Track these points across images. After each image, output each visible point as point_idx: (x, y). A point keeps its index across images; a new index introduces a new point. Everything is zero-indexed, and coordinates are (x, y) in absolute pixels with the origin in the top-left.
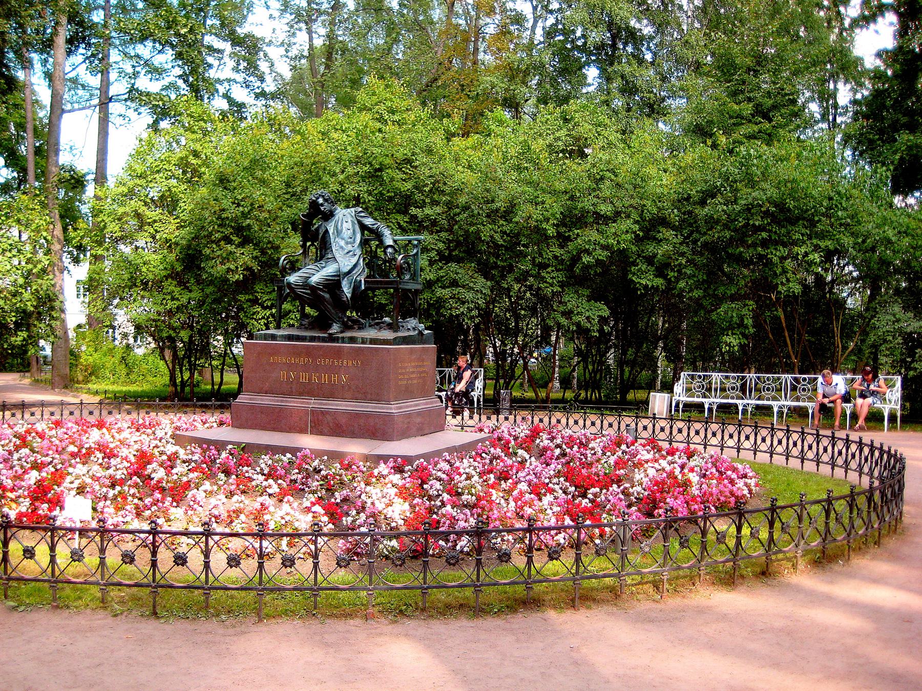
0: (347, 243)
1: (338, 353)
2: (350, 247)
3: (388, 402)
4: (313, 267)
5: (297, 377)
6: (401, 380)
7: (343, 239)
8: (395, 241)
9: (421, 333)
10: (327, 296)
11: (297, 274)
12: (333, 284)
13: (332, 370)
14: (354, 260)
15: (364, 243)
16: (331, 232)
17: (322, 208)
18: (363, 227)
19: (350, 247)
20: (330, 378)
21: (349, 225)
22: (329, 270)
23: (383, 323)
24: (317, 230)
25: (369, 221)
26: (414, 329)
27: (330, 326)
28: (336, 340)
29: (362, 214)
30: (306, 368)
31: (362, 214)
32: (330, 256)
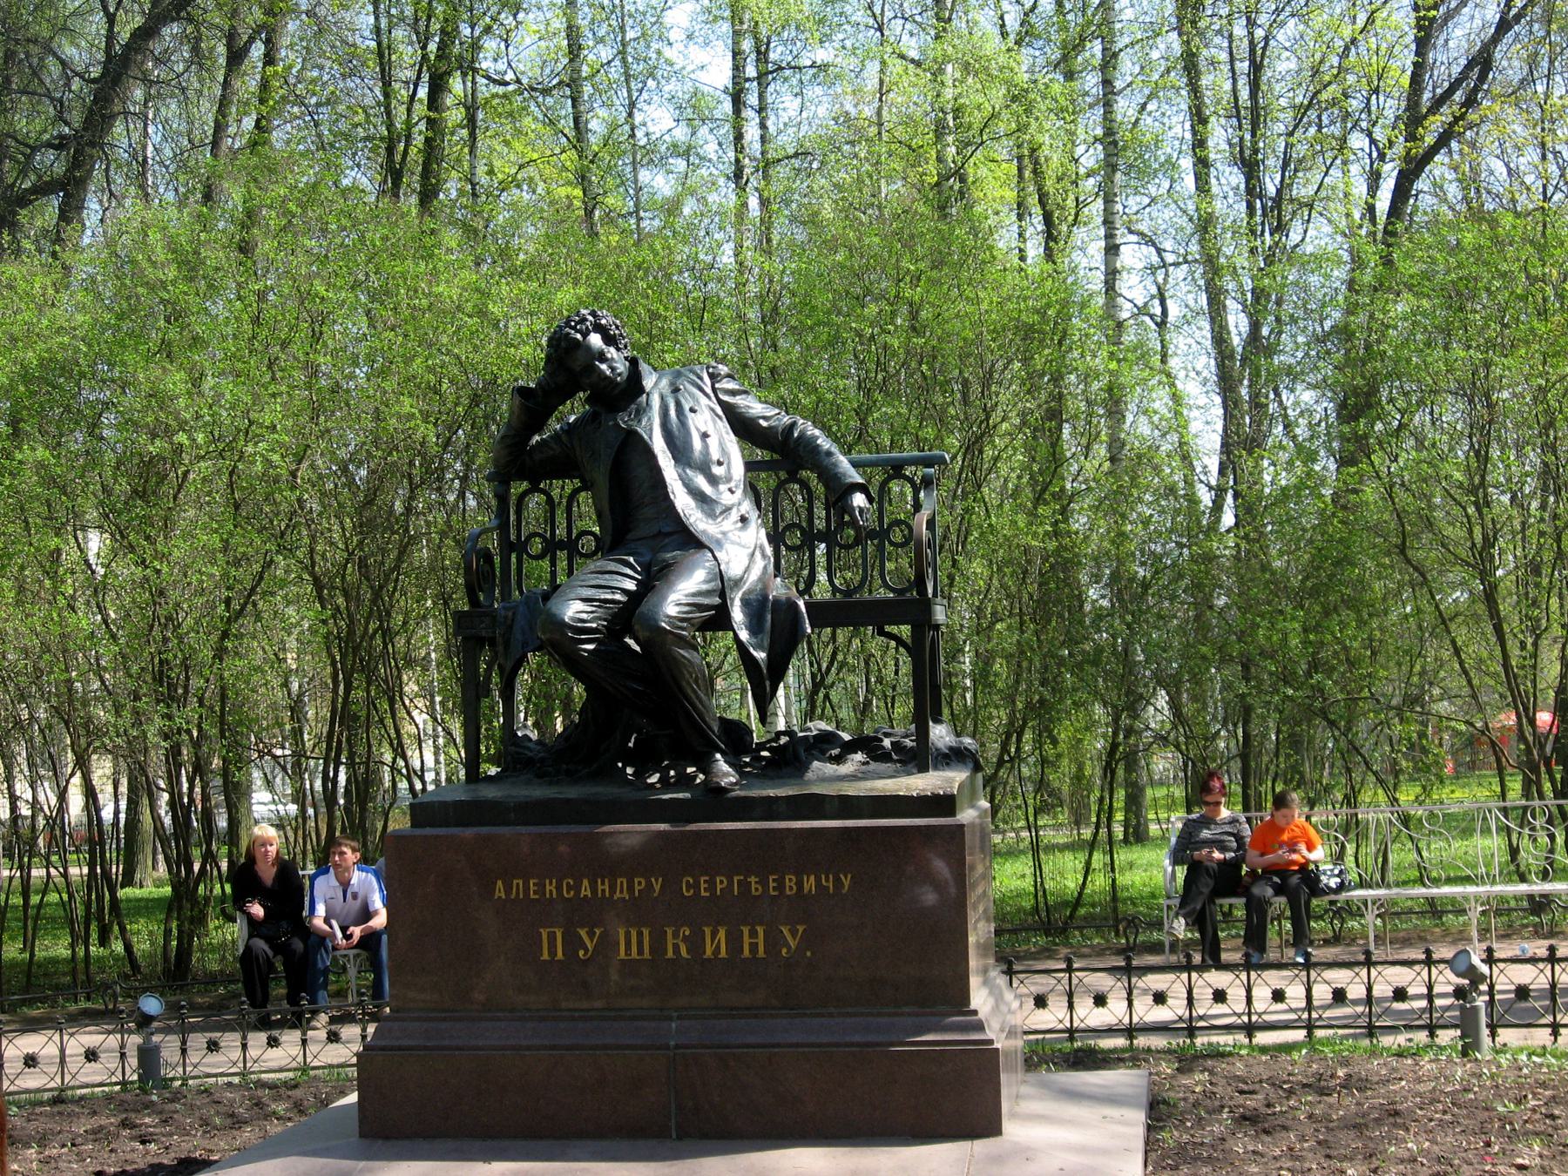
13: (737, 911)
25: (754, 407)
28: (745, 808)
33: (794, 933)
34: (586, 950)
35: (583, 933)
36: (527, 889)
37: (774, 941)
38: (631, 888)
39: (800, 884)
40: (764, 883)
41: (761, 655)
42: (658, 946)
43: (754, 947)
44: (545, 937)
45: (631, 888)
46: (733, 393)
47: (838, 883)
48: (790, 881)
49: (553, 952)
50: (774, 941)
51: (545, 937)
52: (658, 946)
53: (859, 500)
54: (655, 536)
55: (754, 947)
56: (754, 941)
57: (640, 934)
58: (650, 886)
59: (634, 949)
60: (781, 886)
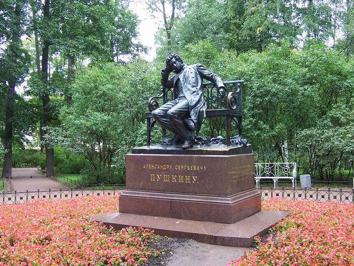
0: (193, 86)
1: (190, 162)
2: (194, 89)
3: (226, 195)
4: (171, 103)
6: (234, 179)
7: (190, 84)
8: (224, 84)
9: (245, 145)
10: (181, 122)
11: (159, 108)
12: (185, 114)
14: (197, 98)
15: (204, 86)
16: (181, 79)
17: (175, 65)
18: (203, 76)
19: (194, 89)
20: (184, 178)
21: (193, 75)
22: (181, 104)
23: (218, 139)
24: (172, 80)
26: (241, 143)
27: (183, 143)
29: (202, 68)
30: (168, 172)
31: (202, 68)
32: (181, 96)
33: (195, 178)
40: (190, 167)
42: (171, 179)
47: (204, 168)
50: (192, 179)
56: (188, 178)
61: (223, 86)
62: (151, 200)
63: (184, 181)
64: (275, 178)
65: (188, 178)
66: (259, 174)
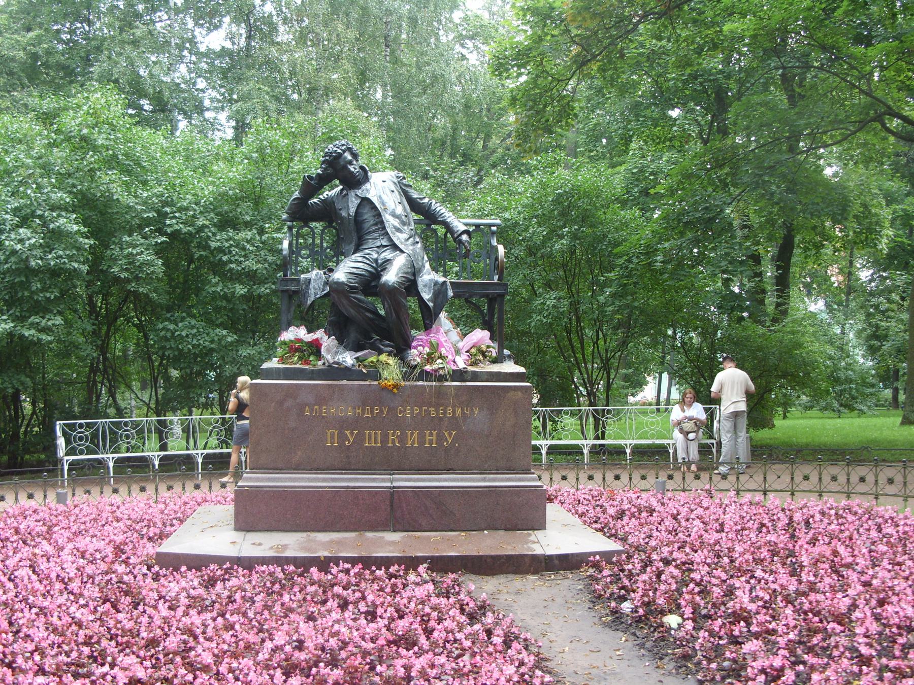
5: (360, 439)
8: (466, 225)
17: (351, 168)
20: (422, 437)
25: (415, 195)
34: (349, 441)
35: (348, 433)
36: (321, 411)
37: (441, 438)
38: (372, 412)
39: (454, 412)
40: (437, 411)
41: (431, 304)
42: (385, 440)
43: (431, 442)
44: (329, 434)
45: (372, 412)
46: (405, 185)
48: (450, 410)
49: (332, 443)
50: (441, 438)
51: (329, 434)
52: (385, 440)
53: (465, 237)
54: (378, 247)
55: (431, 442)
56: (431, 438)
57: (376, 433)
58: (381, 411)
59: (373, 440)
60: (445, 413)
61: (464, 228)
62: (336, 494)
63: (422, 442)
64: (110, 458)
65: (431, 438)
66: (104, 446)
